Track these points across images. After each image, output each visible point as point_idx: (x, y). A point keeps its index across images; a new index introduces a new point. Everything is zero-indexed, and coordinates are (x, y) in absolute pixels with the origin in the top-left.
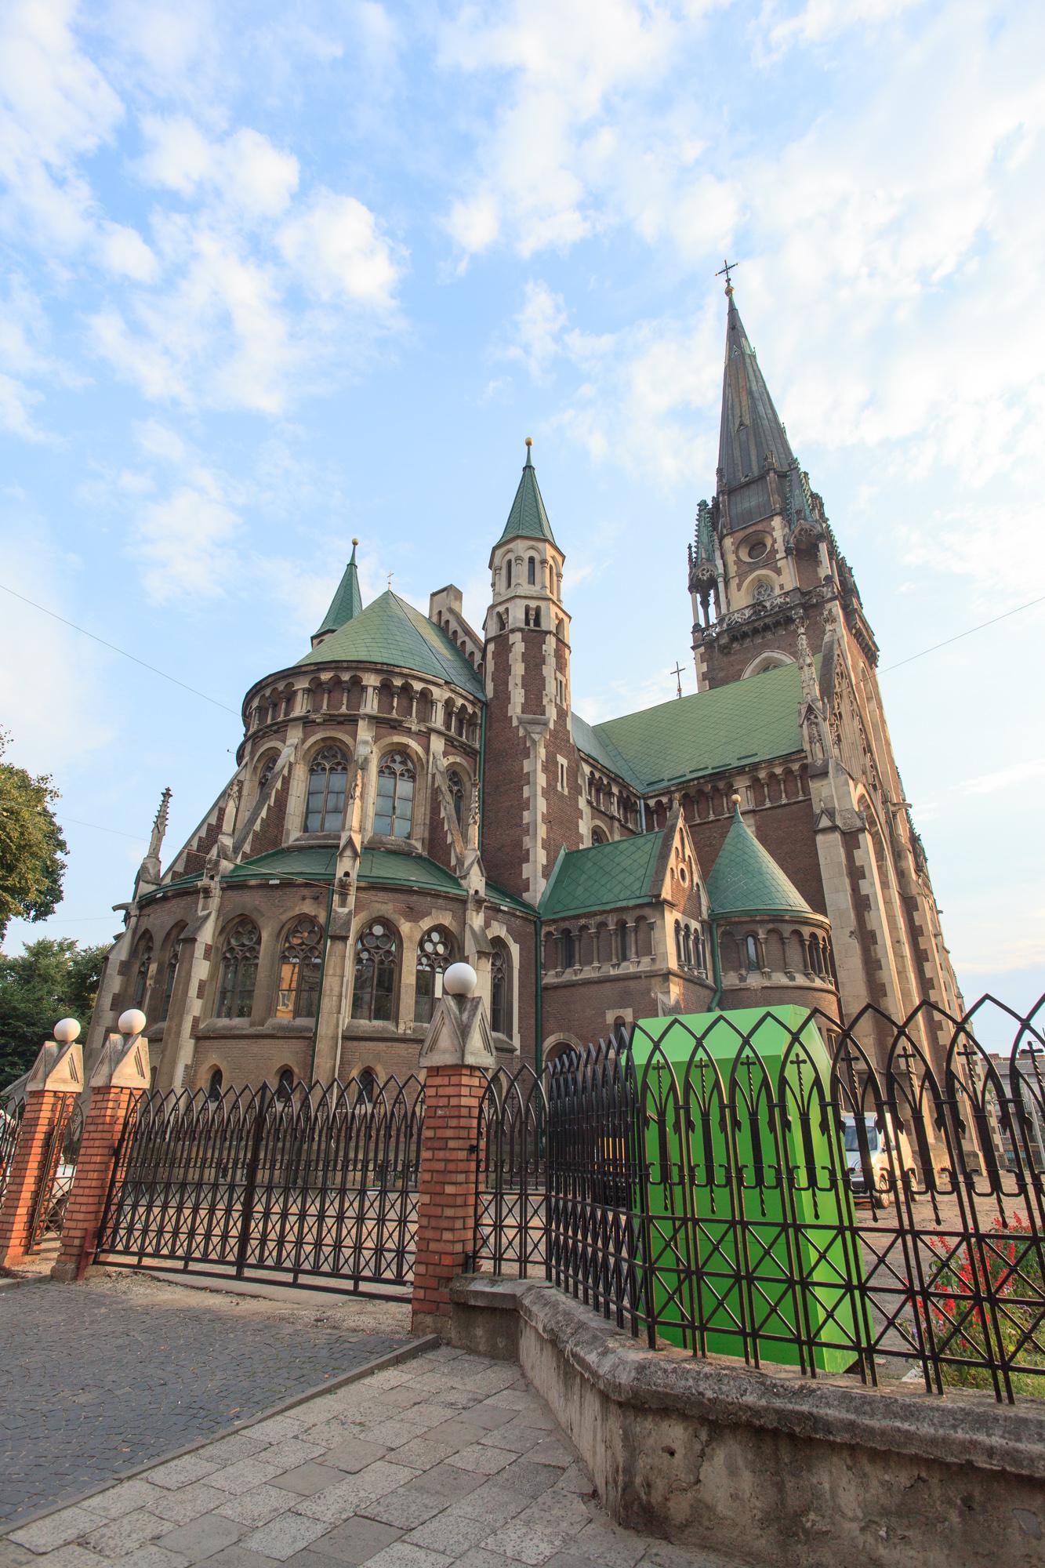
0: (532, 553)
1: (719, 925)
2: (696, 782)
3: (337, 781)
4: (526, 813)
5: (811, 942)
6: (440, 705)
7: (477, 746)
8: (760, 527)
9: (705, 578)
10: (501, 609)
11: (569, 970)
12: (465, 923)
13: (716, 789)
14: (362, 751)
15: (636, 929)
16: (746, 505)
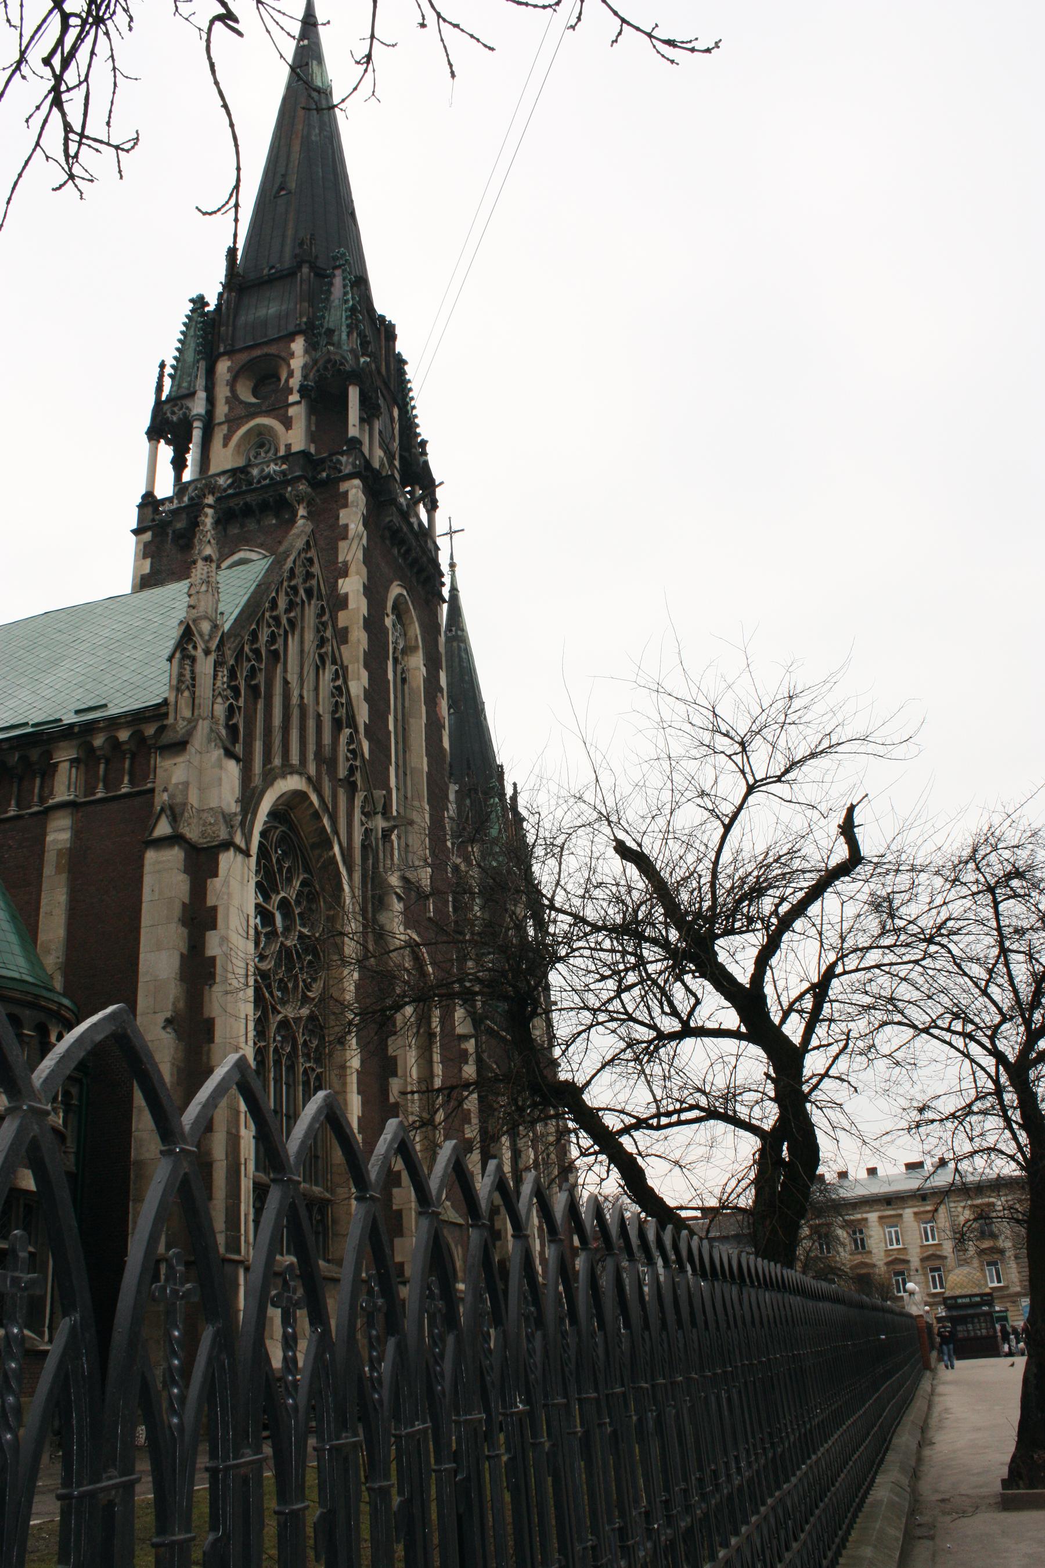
8: (272, 350)
9: (175, 419)
16: (262, 312)
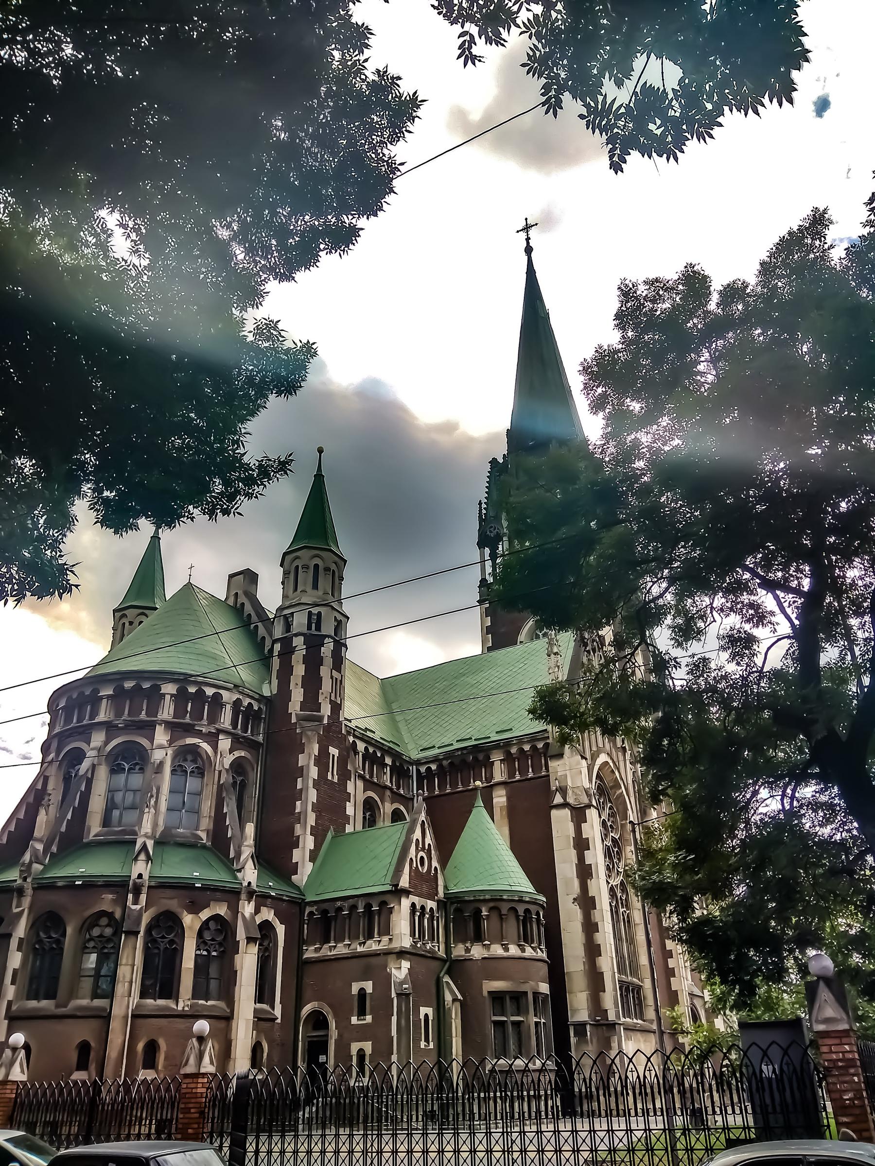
0: (317, 561)
1: (452, 903)
2: (460, 753)
3: (136, 780)
4: (298, 803)
5: (525, 917)
6: (228, 707)
7: (260, 738)
10: (286, 612)
11: (326, 946)
12: (238, 912)
13: (476, 759)
14: (157, 756)
15: (379, 912)
